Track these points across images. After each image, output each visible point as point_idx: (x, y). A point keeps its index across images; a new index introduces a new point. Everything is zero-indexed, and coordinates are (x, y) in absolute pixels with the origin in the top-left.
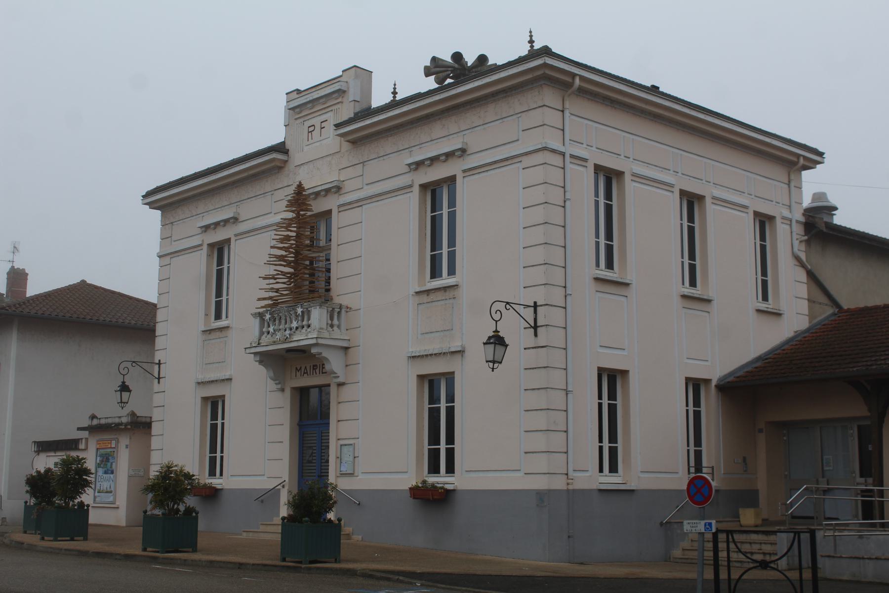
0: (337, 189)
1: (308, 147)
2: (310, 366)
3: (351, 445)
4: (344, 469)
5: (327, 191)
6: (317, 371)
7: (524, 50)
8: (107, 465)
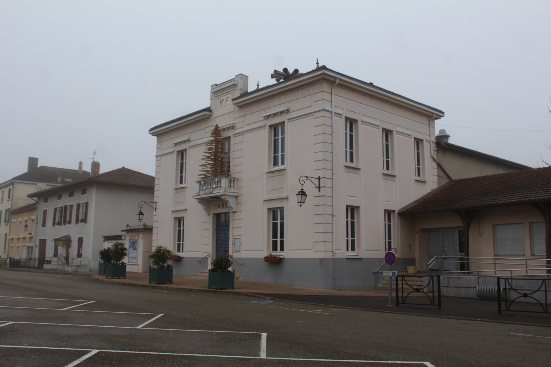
0: (233, 127)
4: (236, 249)
5: (229, 128)
6: (224, 206)
7: (315, 67)
8: (133, 246)
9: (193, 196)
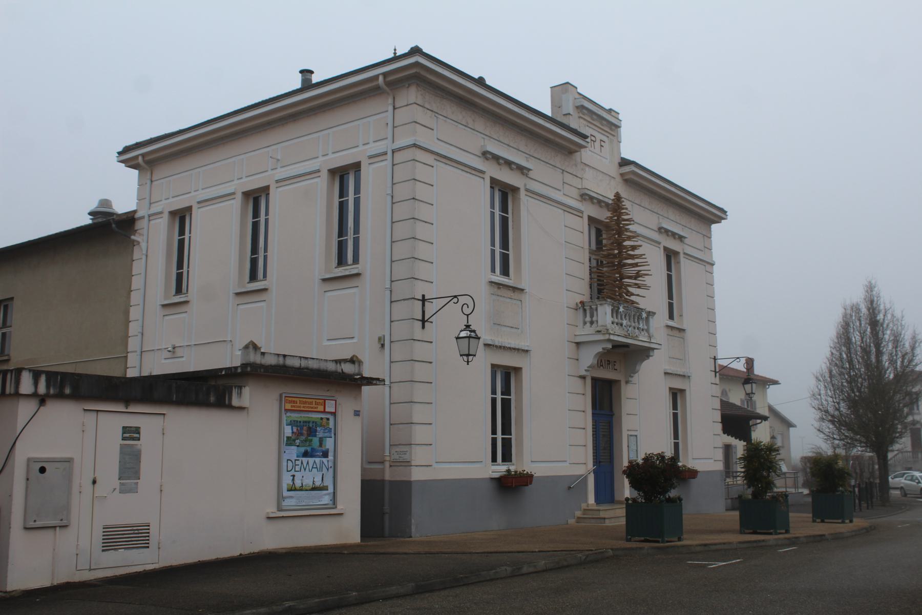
8: (311, 441)
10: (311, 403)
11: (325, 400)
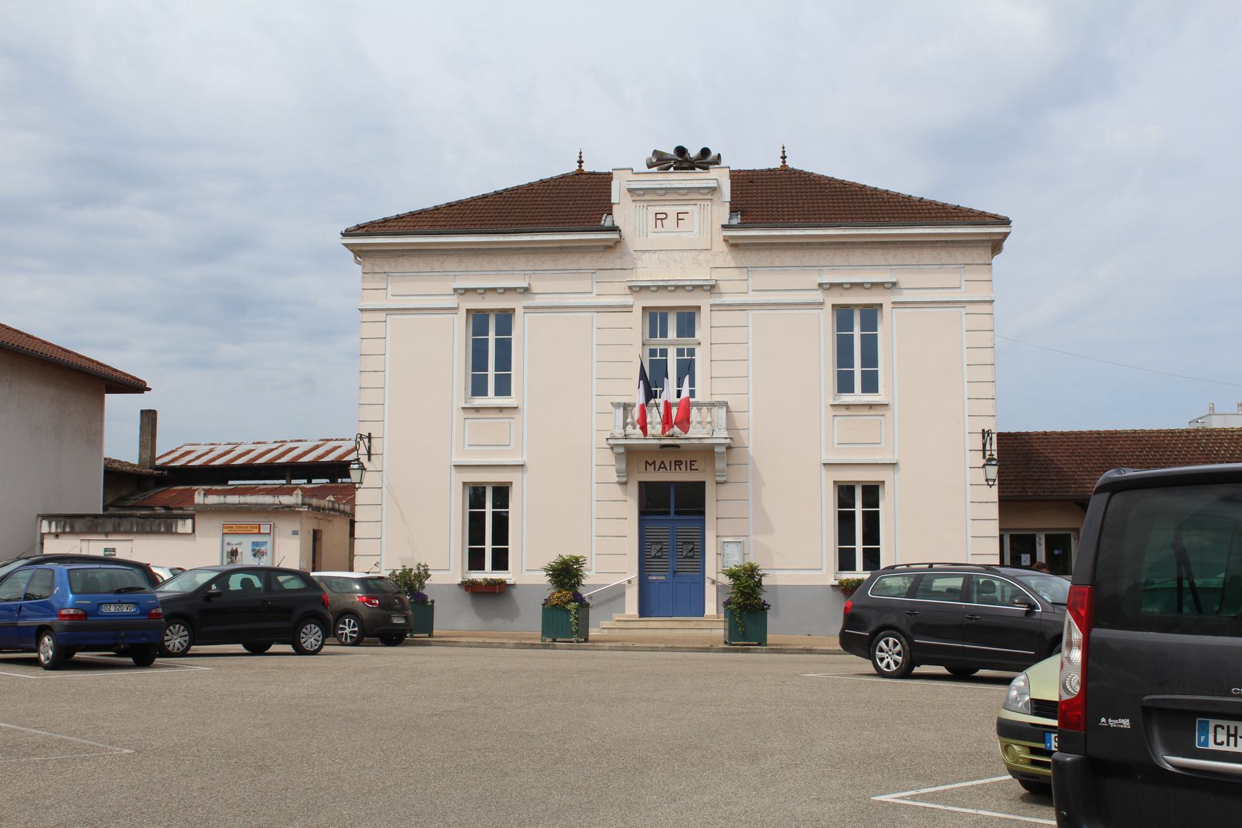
0: (712, 288)
1: (654, 234)
2: (670, 462)
3: (741, 542)
6: (683, 467)
9: (607, 439)
10: (247, 527)
11: (260, 525)
